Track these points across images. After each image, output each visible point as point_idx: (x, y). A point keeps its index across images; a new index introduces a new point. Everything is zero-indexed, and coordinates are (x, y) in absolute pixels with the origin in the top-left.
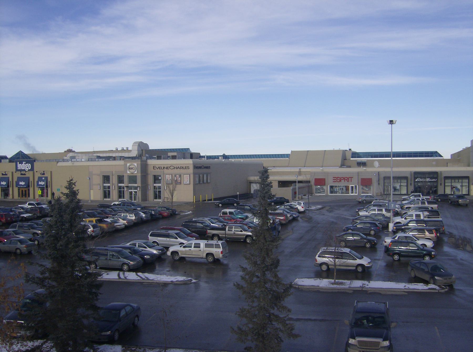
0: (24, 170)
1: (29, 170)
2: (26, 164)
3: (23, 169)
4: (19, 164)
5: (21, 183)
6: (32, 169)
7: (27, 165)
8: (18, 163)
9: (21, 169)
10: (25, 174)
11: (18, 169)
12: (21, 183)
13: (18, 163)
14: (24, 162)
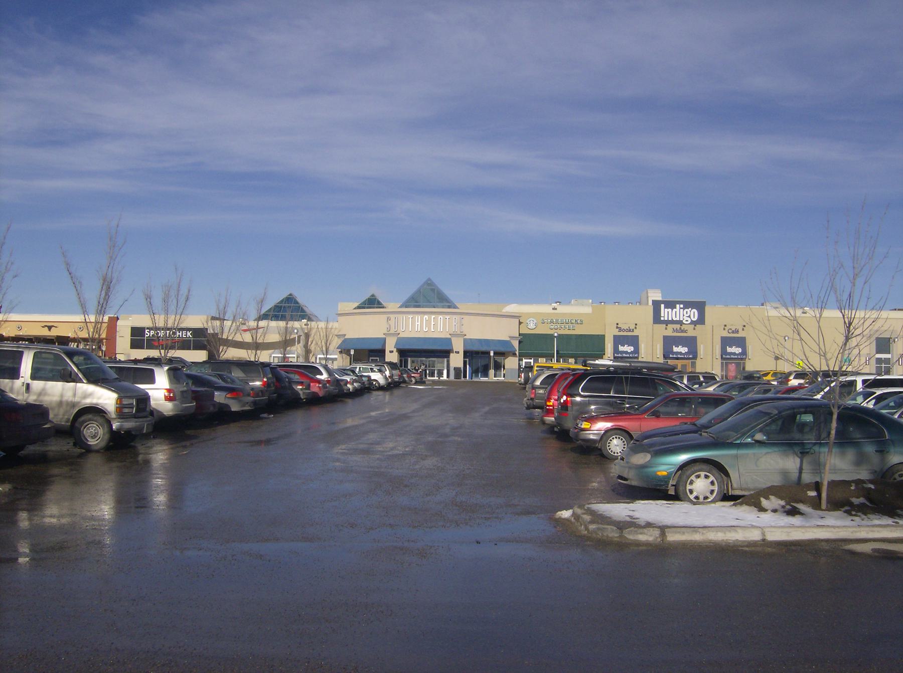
0: (680, 323)
1: (692, 322)
2: (684, 309)
3: (674, 319)
4: (665, 308)
6: (701, 320)
7: (687, 313)
8: (662, 306)
9: (670, 319)
10: (685, 331)
11: (662, 319)
13: (662, 306)
14: (678, 306)
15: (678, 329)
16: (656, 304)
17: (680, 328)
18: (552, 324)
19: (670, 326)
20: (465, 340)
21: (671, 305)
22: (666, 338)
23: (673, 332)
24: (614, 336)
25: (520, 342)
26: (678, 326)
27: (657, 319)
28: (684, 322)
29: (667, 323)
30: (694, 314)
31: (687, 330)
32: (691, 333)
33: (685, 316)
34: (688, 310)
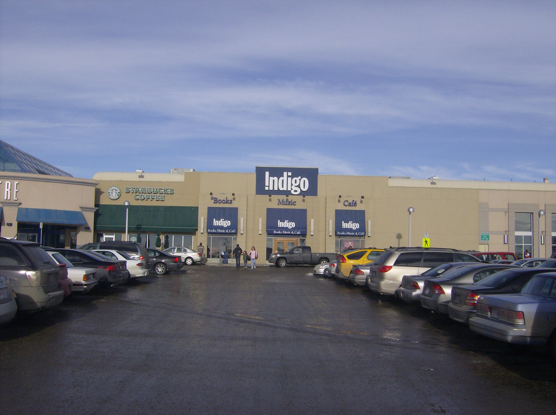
0: (287, 193)
1: (303, 193)
2: (292, 177)
3: (281, 189)
5: (280, 224)
6: (313, 191)
7: (296, 182)
8: (267, 174)
9: (276, 189)
10: (294, 203)
11: (267, 188)
12: (280, 224)
13: (267, 174)
14: (285, 173)
15: (285, 200)
16: (260, 172)
17: (287, 200)
18: (138, 194)
19: (275, 198)
20: (20, 210)
21: (277, 172)
22: (269, 211)
23: (278, 204)
24: (208, 208)
25: (97, 215)
26: (284, 197)
27: (261, 189)
28: (292, 192)
29: (271, 193)
30: (304, 183)
31: (295, 202)
32: (300, 205)
33: (293, 187)
34: (298, 179)
